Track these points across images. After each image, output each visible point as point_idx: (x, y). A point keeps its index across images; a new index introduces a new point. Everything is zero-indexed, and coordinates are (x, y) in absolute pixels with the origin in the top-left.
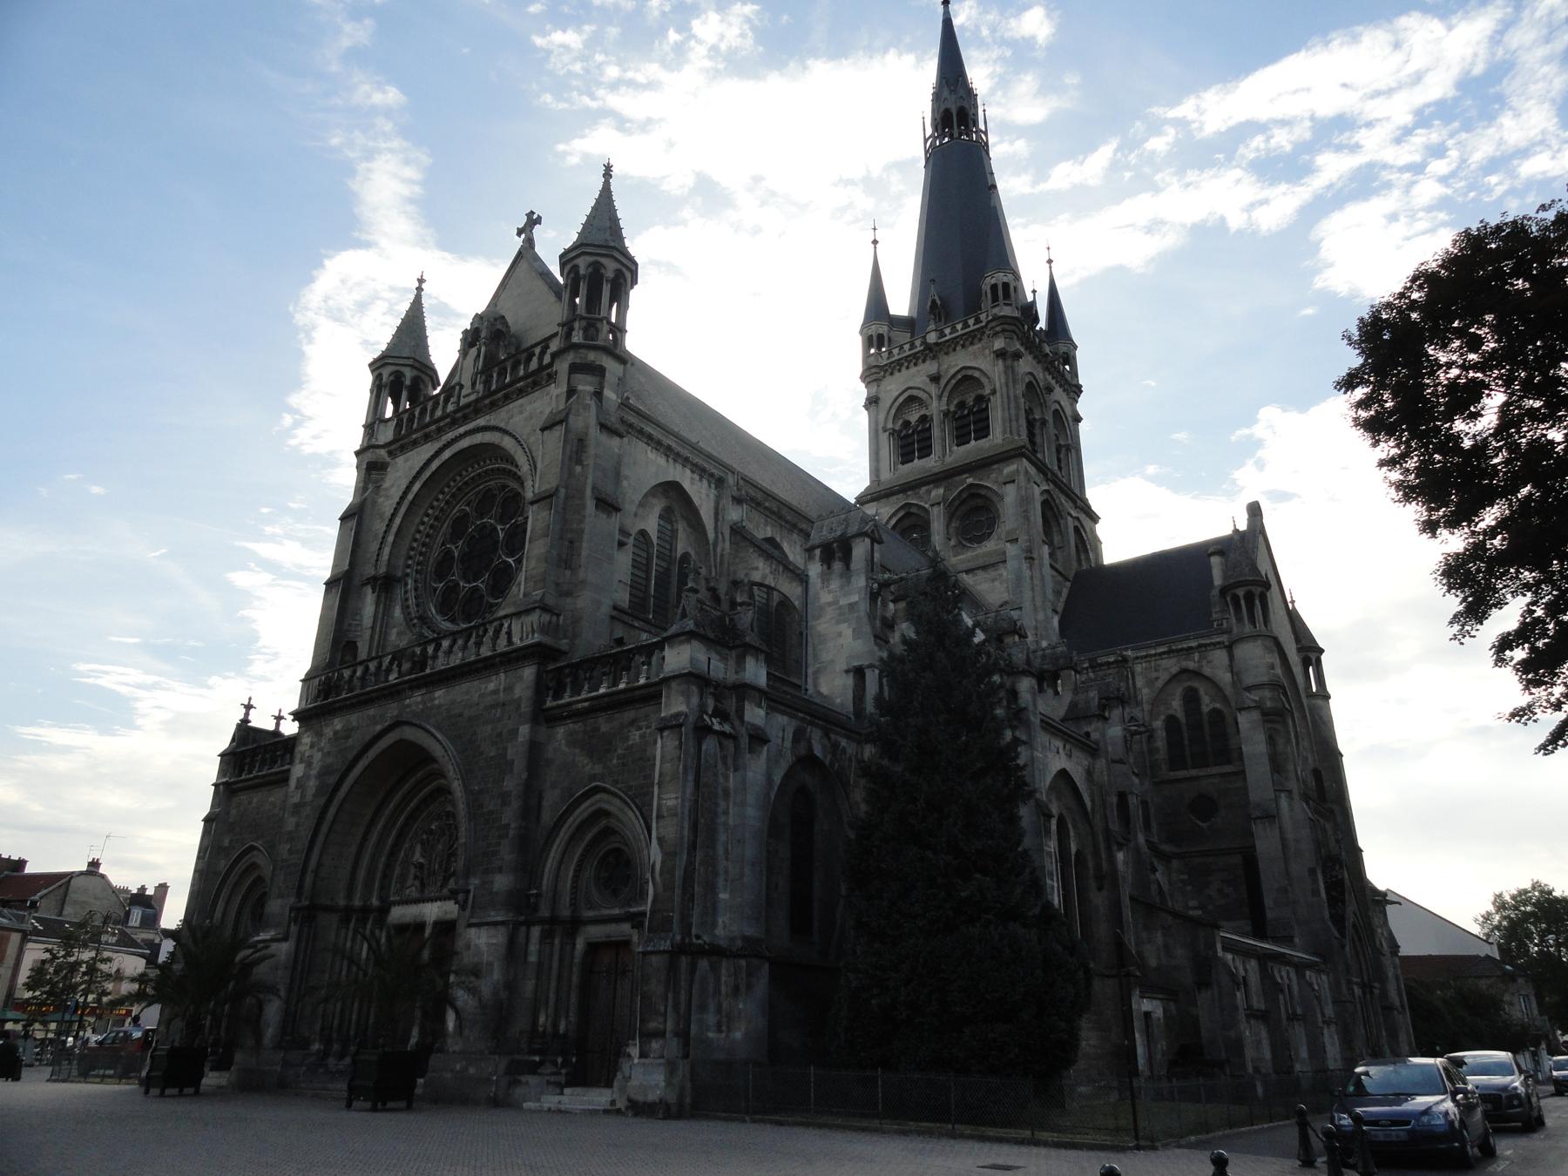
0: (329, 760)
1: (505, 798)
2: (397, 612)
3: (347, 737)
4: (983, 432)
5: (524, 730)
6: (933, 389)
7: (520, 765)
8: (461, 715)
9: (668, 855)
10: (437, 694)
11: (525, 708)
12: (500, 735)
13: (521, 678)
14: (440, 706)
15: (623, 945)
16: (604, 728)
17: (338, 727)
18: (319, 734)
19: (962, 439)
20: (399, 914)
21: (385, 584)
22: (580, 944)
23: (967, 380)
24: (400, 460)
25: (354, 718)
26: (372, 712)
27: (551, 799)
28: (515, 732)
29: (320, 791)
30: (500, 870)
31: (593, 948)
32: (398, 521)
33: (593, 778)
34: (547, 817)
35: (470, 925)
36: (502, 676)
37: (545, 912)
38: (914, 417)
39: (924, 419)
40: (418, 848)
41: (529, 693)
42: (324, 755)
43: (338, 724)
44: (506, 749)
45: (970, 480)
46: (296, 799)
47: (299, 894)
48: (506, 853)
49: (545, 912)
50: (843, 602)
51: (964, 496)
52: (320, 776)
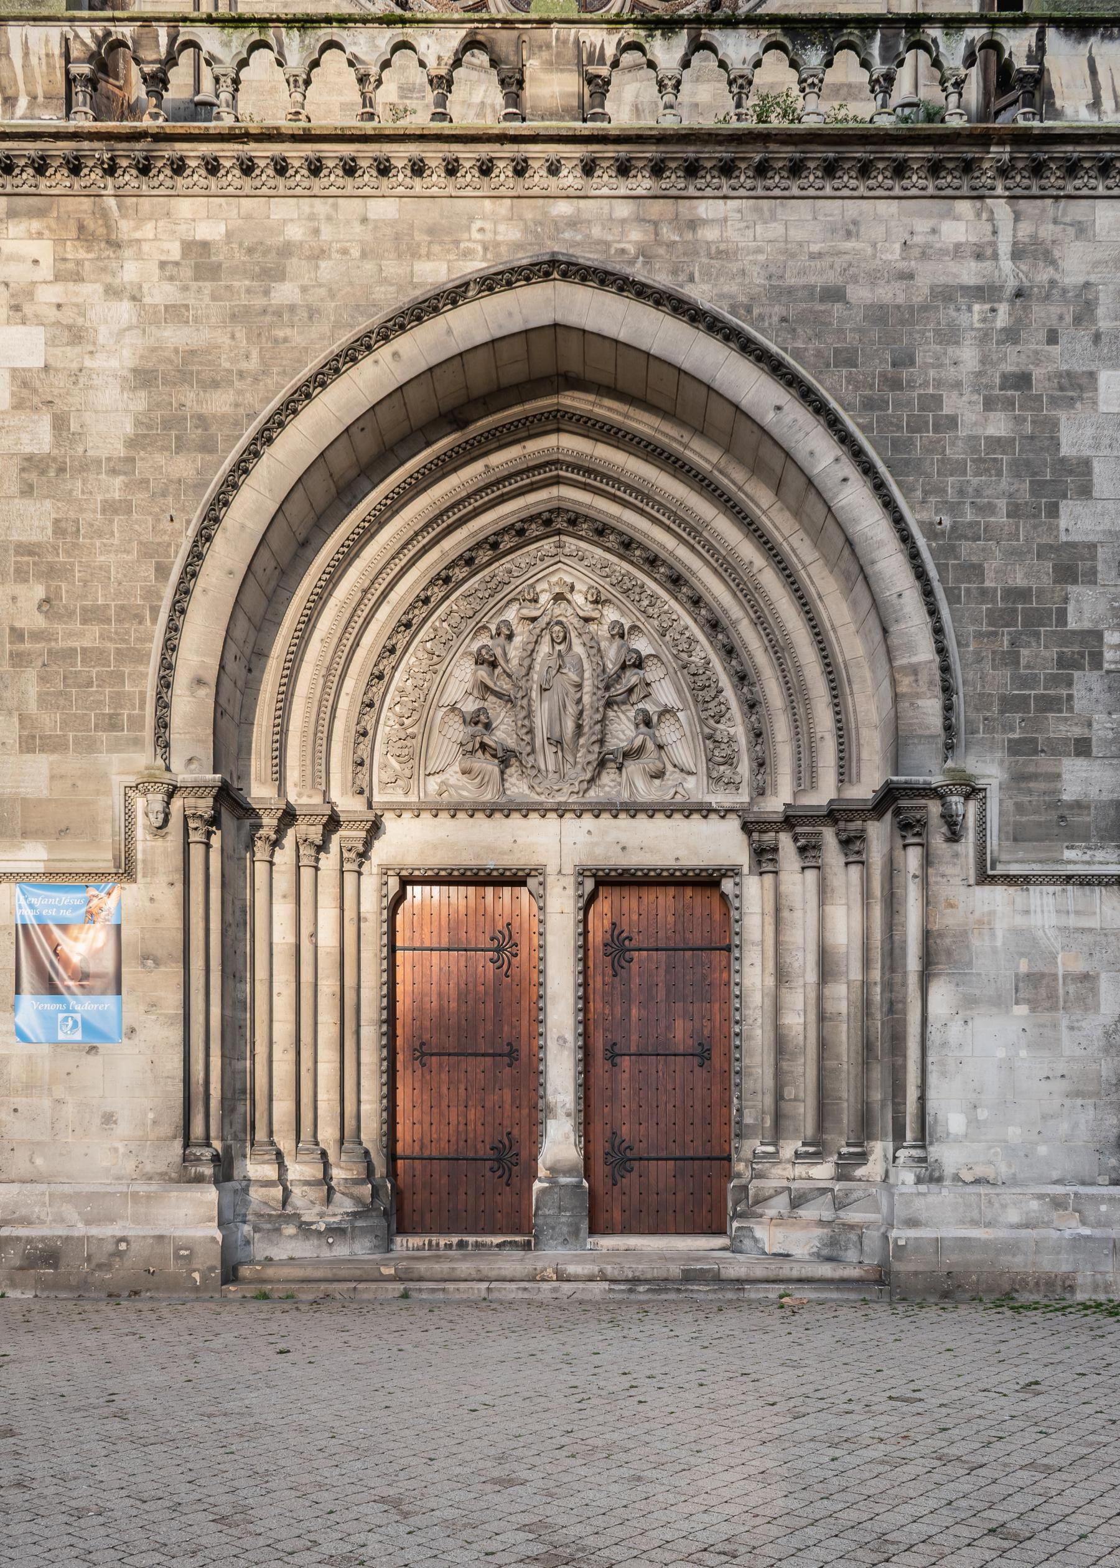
0: (174, 337)
3: (272, 274)
8: (835, 294)
10: (705, 209)
12: (1022, 380)
13: (1082, 230)
14: (723, 254)
17: (210, 231)
25: (287, 214)
26: (383, 209)
29: (163, 430)
30: (1082, 748)
35: (985, 878)
36: (1002, 209)
42: (152, 317)
44: (1055, 424)
46: (38, 437)
47: (163, 744)
52: (143, 378)
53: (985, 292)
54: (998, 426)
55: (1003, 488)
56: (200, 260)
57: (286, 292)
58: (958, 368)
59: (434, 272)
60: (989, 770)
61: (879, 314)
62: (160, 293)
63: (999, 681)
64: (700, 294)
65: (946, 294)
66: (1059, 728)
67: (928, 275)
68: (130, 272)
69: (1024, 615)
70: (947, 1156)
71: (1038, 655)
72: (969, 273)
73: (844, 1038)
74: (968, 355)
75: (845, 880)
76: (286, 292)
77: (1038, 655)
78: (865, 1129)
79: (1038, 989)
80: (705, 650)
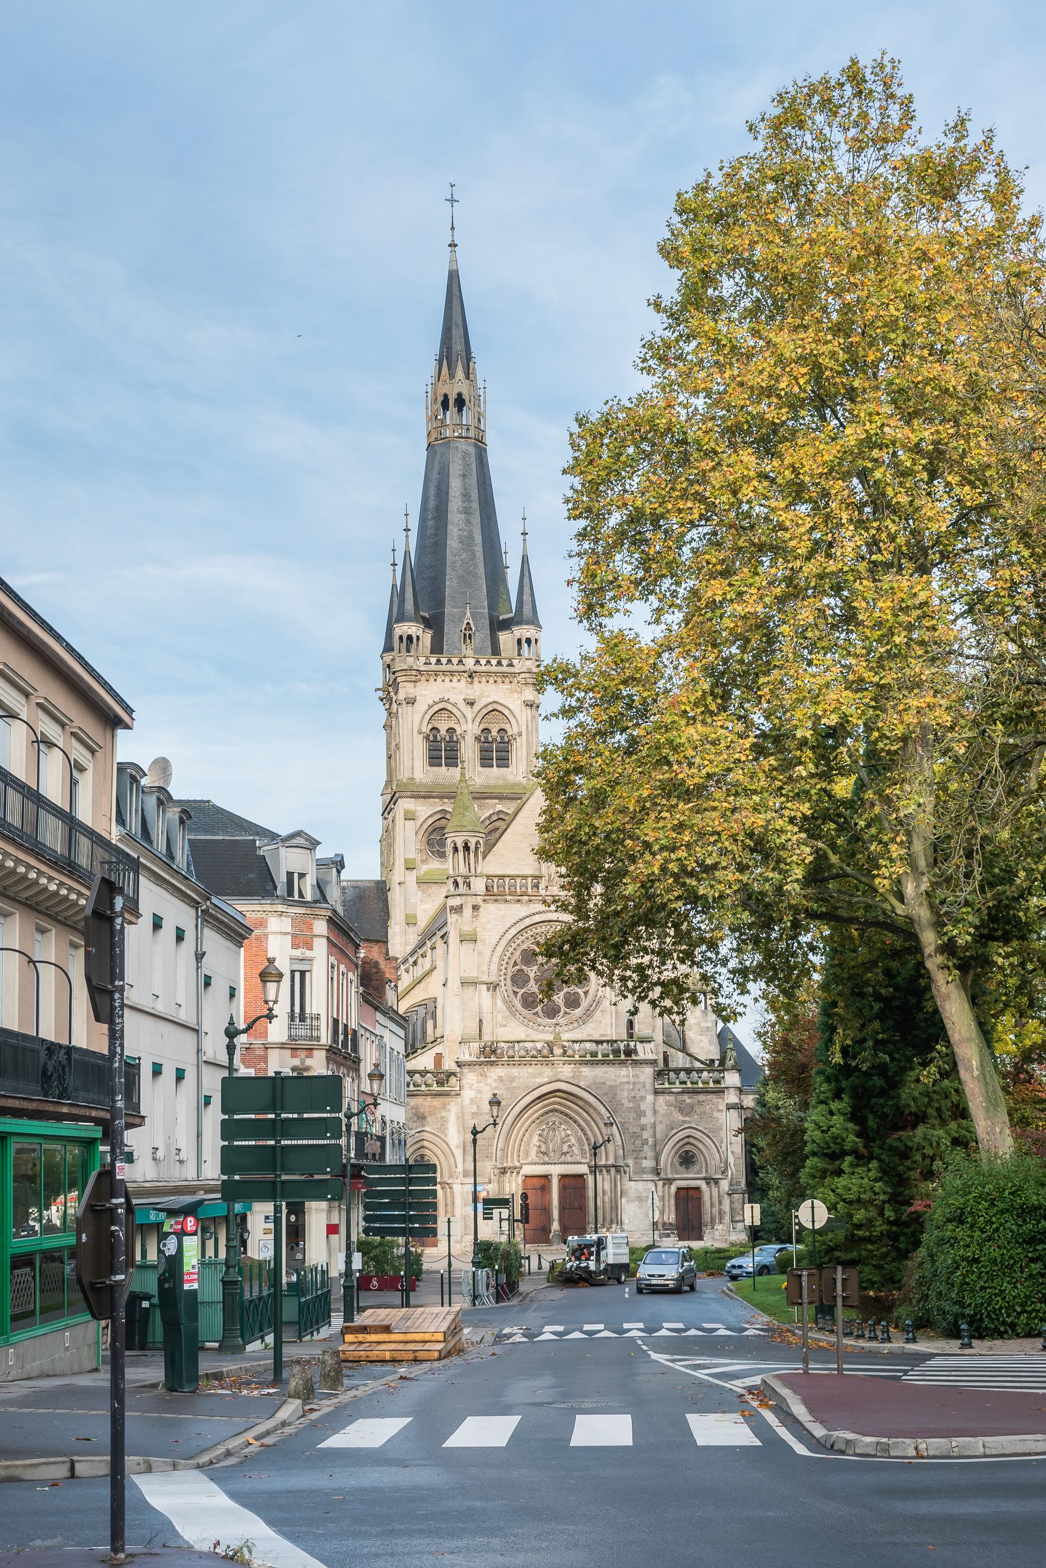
1: (643, 1128)
2: (500, 1003)
4: (504, 761)
5: (650, 1098)
6: (469, 712)
7: (649, 1113)
9: (736, 1159)
11: (649, 1086)
15: (698, 1189)
16: (688, 1101)
18: (484, 1075)
19: (486, 761)
20: (528, 1170)
21: (493, 987)
22: (673, 1189)
23: (494, 711)
24: (491, 907)
25: (515, 1071)
26: (531, 1069)
27: (660, 1128)
28: (643, 1098)
31: (679, 1189)
32: (500, 949)
33: (684, 1122)
34: (659, 1136)
37: (662, 1175)
38: (443, 728)
39: (451, 730)
40: (536, 1138)
41: (651, 1080)
43: (499, 1071)
45: (499, 807)
46: (474, 1109)
48: (648, 1151)
49: (662, 1175)
50: (703, 1025)
51: (495, 818)
53: (628, 1083)
54: (631, 1105)
55: (632, 1115)
56: (501, 1079)
57: (515, 1084)
58: (624, 1095)
59: (539, 1081)
60: (630, 1162)
61: (611, 1087)
62: (494, 1085)
63: (632, 1147)
64: (582, 1084)
65: (622, 1083)
66: (642, 1155)
67: (619, 1080)
68: (489, 1081)
69: (636, 1136)
70: (625, 1227)
71: (638, 1143)
72: (625, 1080)
73: (608, 1206)
74: (626, 1093)
75: (607, 1177)
76: (515, 1084)
77: (638, 1143)
78: (611, 1222)
79: (640, 1199)
80: (580, 1133)
